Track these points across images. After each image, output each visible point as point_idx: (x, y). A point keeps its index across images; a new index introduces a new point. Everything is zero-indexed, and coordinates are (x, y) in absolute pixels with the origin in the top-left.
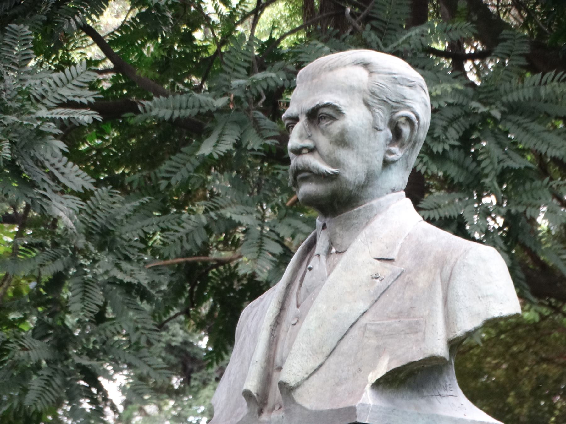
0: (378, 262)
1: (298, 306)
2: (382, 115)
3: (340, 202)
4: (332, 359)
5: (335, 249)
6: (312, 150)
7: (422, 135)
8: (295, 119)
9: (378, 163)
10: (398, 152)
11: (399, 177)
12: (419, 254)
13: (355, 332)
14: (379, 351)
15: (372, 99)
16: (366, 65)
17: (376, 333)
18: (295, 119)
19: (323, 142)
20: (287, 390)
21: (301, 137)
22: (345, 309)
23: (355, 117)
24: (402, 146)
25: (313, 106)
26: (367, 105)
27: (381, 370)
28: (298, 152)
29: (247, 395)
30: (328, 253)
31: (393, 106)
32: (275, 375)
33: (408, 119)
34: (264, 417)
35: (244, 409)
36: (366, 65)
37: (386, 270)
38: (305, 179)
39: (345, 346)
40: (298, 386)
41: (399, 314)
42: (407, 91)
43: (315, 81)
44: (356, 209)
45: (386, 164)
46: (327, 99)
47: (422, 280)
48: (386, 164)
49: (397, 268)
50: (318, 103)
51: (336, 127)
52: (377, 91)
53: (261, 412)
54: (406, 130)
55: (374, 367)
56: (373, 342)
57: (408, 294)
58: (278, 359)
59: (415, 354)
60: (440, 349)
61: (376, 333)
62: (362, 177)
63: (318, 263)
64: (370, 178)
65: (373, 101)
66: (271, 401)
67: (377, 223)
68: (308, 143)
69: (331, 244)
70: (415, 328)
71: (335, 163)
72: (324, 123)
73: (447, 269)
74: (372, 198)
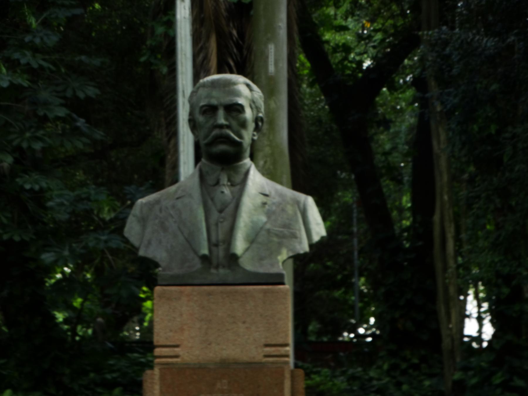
0: (262, 196)
1: (221, 211)
4: (254, 245)
6: (229, 127)
14: (280, 245)
17: (277, 235)
19: (234, 124)
22: (255, 218)
25: (231, 103)
28: (221, 127)
36: (248, 85)
43: (227, 89)
44: (241, 163)
47: (290, 209)
50: (234, 102)
52: (255, 100)
55: (279, 253)
56: (275, 239)
58: (214, 239)
61: (277, 235)
65: (253, 106)
66: (215, 262)
71: (241, 137)
72: (234, 114)
73: (302, 206)
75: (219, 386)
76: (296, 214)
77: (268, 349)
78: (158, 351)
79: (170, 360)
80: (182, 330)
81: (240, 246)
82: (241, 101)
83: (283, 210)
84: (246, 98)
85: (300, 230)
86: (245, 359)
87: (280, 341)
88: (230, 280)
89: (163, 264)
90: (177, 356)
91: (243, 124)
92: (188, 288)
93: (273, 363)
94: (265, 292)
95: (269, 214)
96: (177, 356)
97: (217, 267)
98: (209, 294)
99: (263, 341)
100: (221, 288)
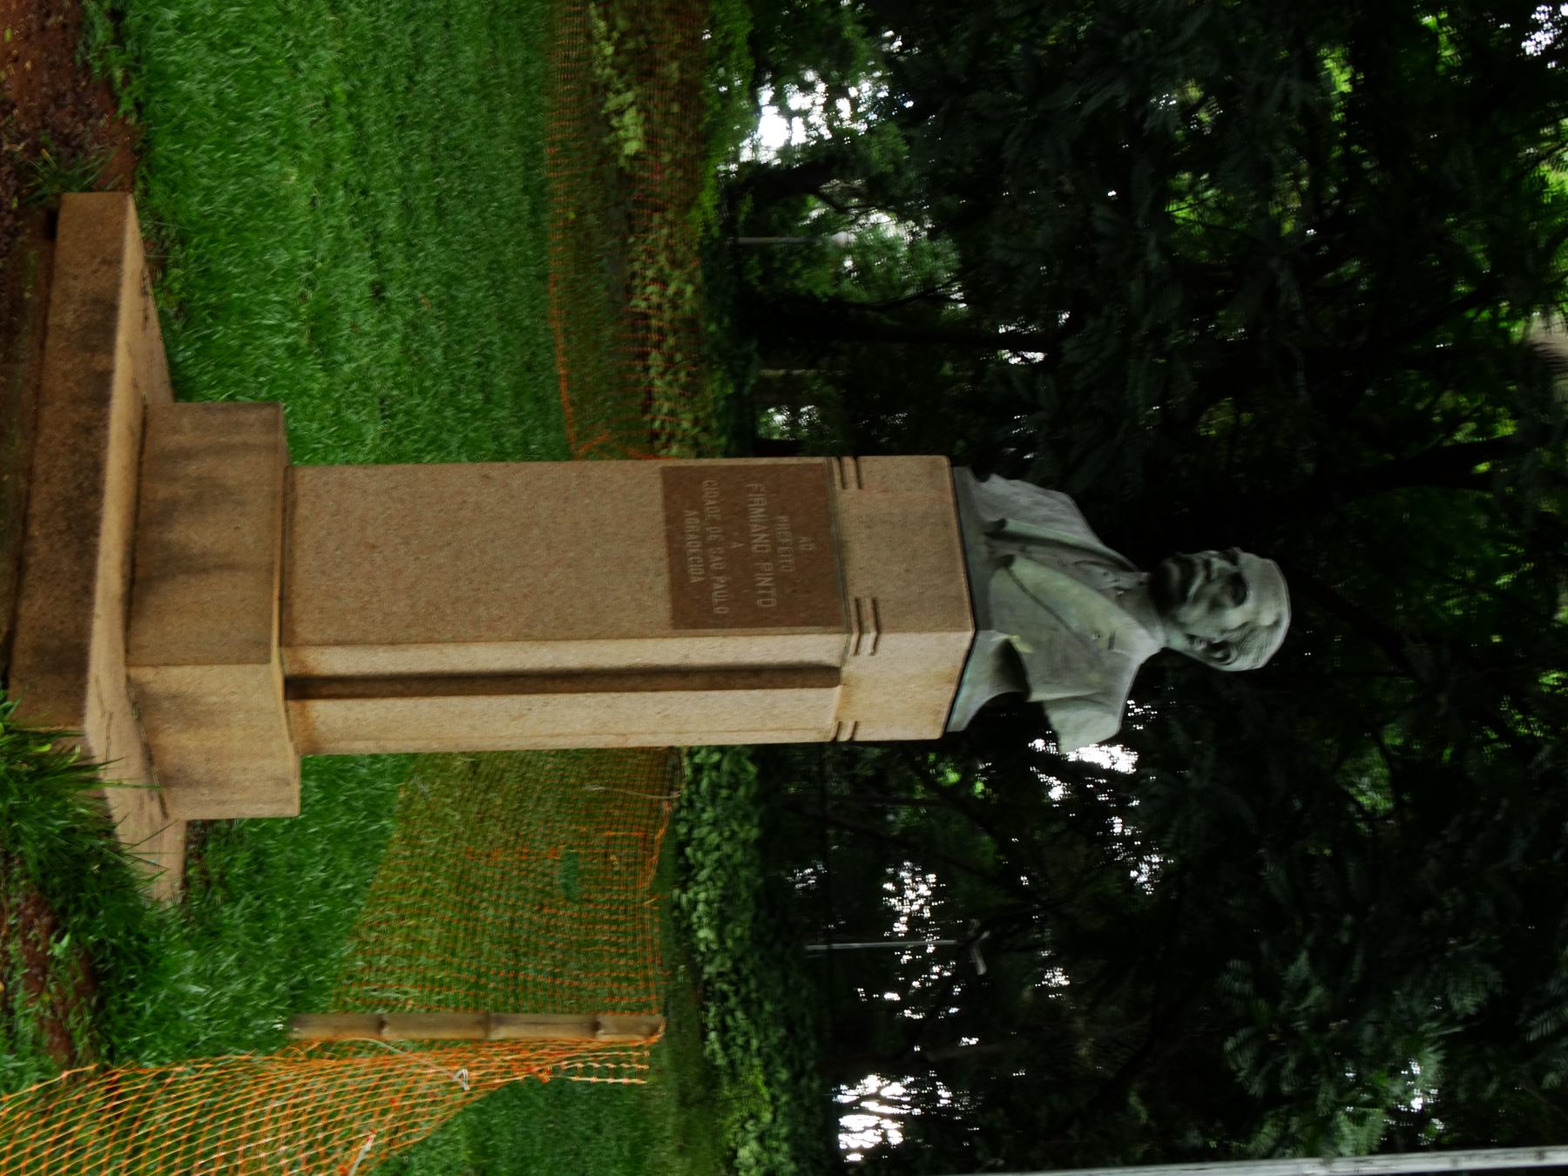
2: (1235, 636)
3: (1161, 601)
4: (1028, 601)
5: (1121, 597)
6: (1208, 579)
7: (1214, 665)
8: (1233, 560)
9: (1193, 631)
10: (1200, 647)
11: (1179, 643)
12: (1114, 672)
13: (1053, 621)
14: (1036, 644)
15: (1249, 629)
16: (1277, 624)
17: (1051, 641)
18: (1233, 560)
19: (1214, 588)
20: (1007, 562)
21: (1221, 570)
22: (1073, 611)
23: (1234, 617)
24: (1205, 650)
26: (1244, 625)
27: (1023, 648)
28: (1207, 565)
29: (1002, 523)
30: (1118, 588)
31: (1241, 646)
32: (1017, 546)
33: (1227, 657)
34: (983, 538)
35: (992, 518)
36: (1277, 624)
37: (1103, 643)
38: (1183, 571)
39: (1042, 612)
40: (1010, 573)
41: (1066, 660)
42: (1251, 657)
45: (1192, 638)
46: (1251, 594)
47: (1094, 677)
48: (1192, 638)
49: (1104, 654)
51: (1227, 600)
53: (987, 534)
54: (1219, 655)
55: (1024, 640)
57: (1083, 665)
58: (1030, 548)
59: (1033, 676)
60: (1037, 696)
62: (1182, 620)
63: (1109, 580)
64: (1181, 626)
65: (1247, 629)
66: (996, 543)
67: (1142, 632)
68: (1214, 575)
69: (1126, 590)
70: (1054, 676)
71: (1197, 598)
72: (1230, 589)
73: (1101, 699)
74: (1164, 625)
75: (805, 539)
76: (1089, 686)
77: (867, 606)
78: (849, 461)
79: (837, 477)
80: (886, 491)
81: (1025, 570)
82: (1249, 605)
83: (1092, 666)
84: (1257, 613)
85: (1067, 688)
86: (851, 573)
87: (884, 620)
88: (972, 558)
89: (984, 485)
90: (844, 486)
91: (1215, 606)
92: (950, 499)
93: (847, 610)
94: (959, 598)
95: (1081, 638)
96: (844, 486)
97: (987, 544)
98: (947, 525)
99: (881, 597)
100: (957, 540)
